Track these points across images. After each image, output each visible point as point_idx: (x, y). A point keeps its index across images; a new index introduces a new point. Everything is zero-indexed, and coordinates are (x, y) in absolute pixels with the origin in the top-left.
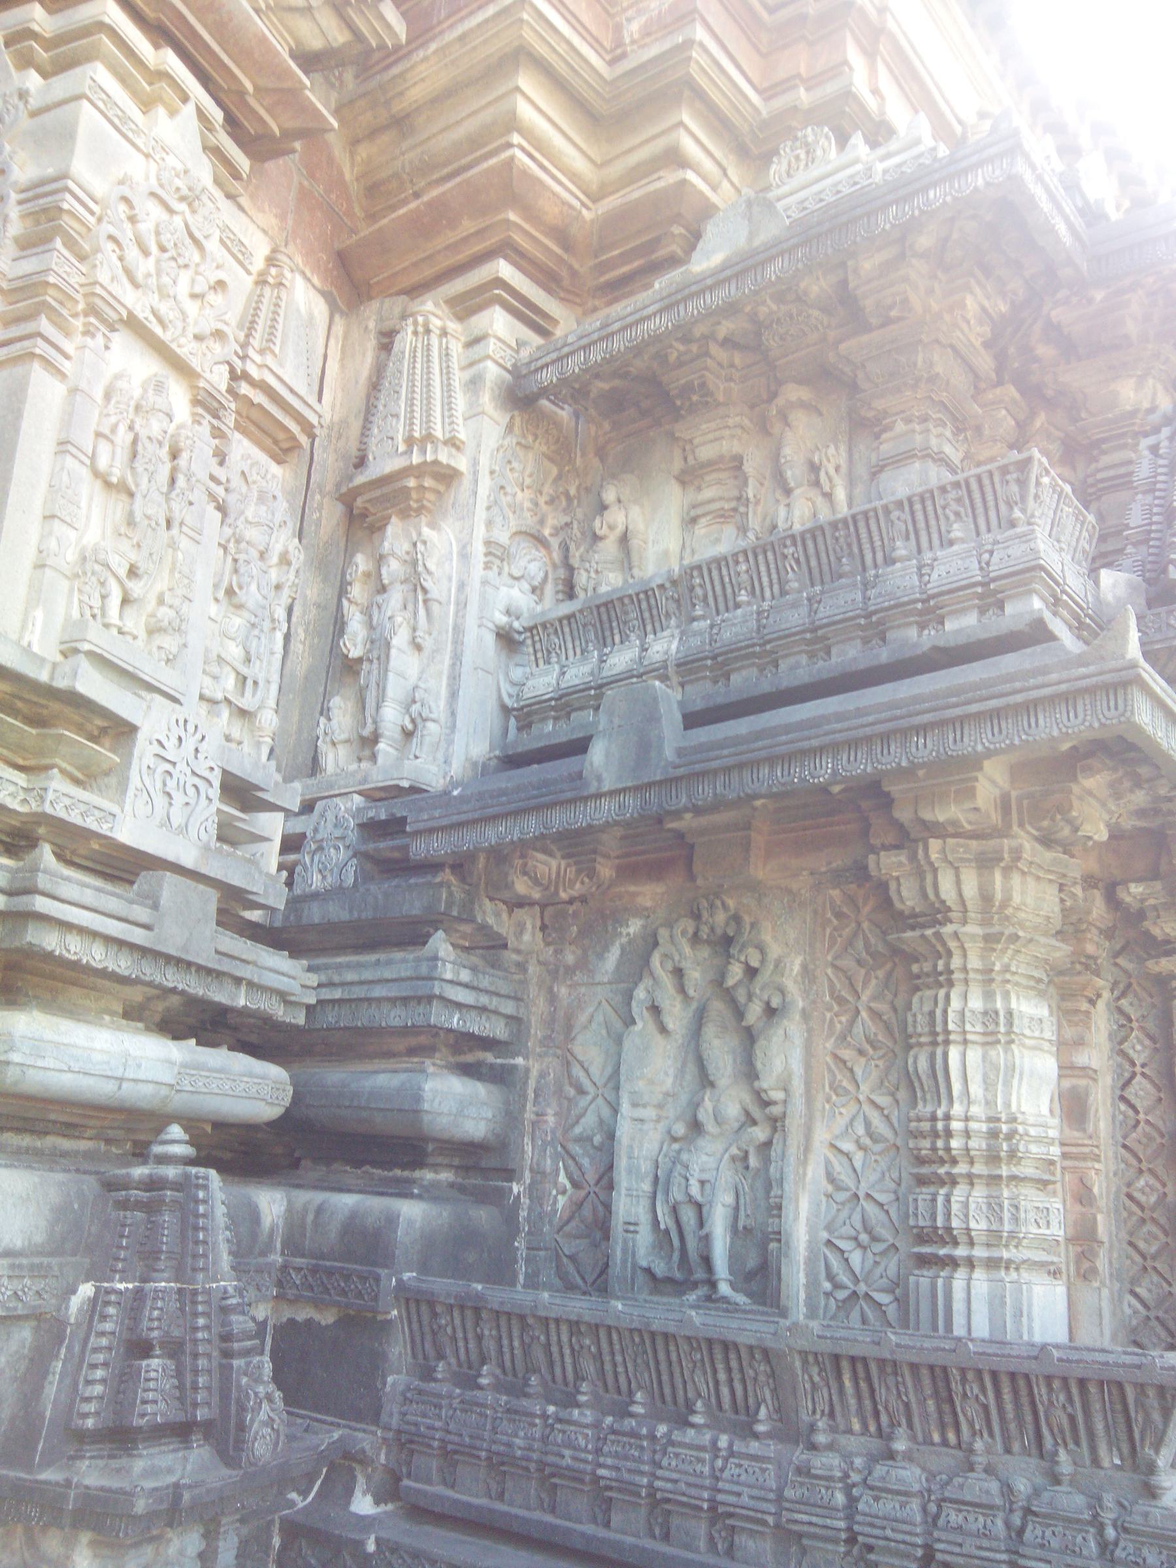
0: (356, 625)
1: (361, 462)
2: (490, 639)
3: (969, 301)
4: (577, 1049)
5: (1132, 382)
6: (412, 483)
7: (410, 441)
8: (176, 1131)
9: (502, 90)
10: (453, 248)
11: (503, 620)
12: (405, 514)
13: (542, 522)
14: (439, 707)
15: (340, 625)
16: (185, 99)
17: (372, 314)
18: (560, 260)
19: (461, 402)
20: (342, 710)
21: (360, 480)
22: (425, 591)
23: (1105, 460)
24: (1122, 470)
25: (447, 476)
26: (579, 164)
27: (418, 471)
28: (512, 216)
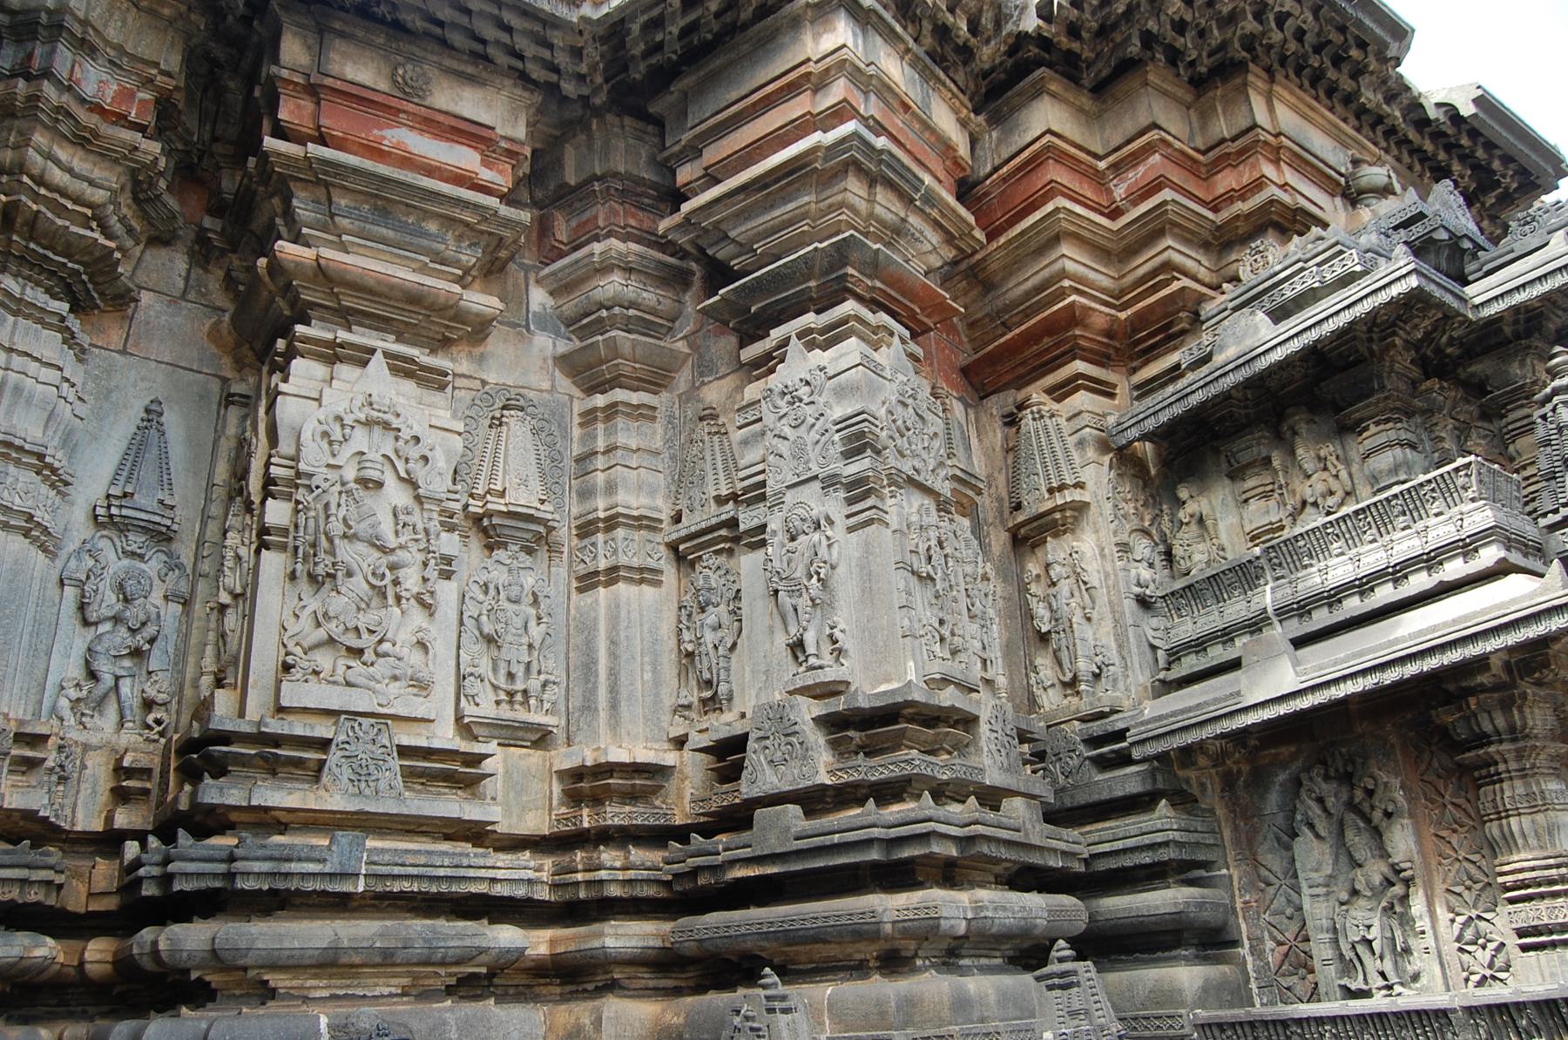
0: (1041, 610)
1: (1018, 507)
2: (1134, 604)
3: (1398, 341)
4: (1260, 858)
5: (1516, 364)
6: (1058, 516)
7: (1051, 491)
8: (1061, 943)
9: (1054, 257)
10: (1040, 354)
11: (1138, 590)
12: (1056, 536)
13: (1142, 519)
14: (1113, 656)
15: (1030, 616)
16: (892, 334)
17: (999, 404)
18: (1107, 345)
19: (1075, 455)
20: (1046, 668)
21: (1021, 518)
22: (1085, 583)
23: (1511, 417)
24: (1525, 422)
25: (1081, 508)
26: (1106, 282)
27: (1061, 508)
28: (1077, 332)
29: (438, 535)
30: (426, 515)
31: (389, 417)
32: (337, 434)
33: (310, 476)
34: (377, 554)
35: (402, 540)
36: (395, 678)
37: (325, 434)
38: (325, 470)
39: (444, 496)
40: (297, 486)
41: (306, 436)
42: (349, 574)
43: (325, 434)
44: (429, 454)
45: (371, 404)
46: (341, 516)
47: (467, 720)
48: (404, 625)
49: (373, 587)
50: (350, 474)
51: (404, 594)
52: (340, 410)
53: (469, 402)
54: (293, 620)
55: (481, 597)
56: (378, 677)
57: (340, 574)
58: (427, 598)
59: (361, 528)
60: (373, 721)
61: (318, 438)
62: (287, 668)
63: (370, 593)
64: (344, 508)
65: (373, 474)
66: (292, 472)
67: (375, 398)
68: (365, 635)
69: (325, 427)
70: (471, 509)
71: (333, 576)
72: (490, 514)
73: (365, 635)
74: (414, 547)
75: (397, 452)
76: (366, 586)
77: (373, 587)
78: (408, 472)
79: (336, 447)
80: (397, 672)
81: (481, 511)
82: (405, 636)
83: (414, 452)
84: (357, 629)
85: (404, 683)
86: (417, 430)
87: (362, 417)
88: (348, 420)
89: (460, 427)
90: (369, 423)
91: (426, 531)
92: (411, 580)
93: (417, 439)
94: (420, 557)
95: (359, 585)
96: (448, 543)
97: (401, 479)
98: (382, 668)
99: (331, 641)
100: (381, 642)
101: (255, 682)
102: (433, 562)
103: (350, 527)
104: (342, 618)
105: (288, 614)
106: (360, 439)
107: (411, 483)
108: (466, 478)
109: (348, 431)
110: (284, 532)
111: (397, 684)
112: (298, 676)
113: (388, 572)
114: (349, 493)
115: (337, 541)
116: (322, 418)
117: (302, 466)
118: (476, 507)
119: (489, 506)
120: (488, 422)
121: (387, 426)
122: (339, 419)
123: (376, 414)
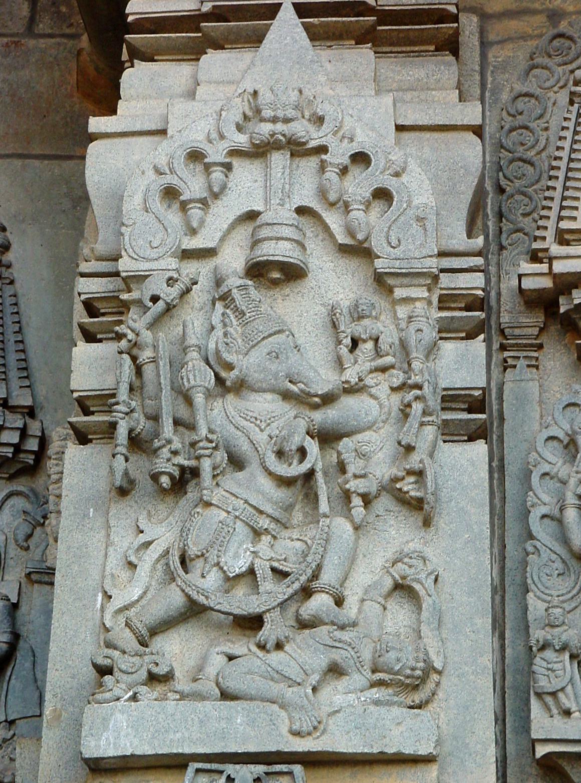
29: (431, 351)
30: (402, 312)
31: (300, 129)
32: (193, 185)
33: (141, 279)
34: (286, 411)
35: (351, 375)
36: (335, 670)
37: (170, 193)
38: (173, 263)
39: (433, 264)
40: (124, 307)
41: (133, 204)
42: (236, 462)
43: (170, 193)
44: (391, 184)
45: (258, 111)
46: (212, 346)
47: (541, 751)
48: (364, 556)
49: (286, 482)
50: (233, 259)
51: (352, 485)
52: (197, 136)
53: (523, 65)
54: (124, 574)
55: (562, 468)
56: (294, 672)
57: (206, 465)
58: (408, 486)
59: (249, 364)
60: (260, 769)
61: (157, 204)
62: (104, 671)
63: (281, 494)
64: (219, 332)
65: (278, 251)
66: (117, 283)
67: (265, 97)
68: (268, 584)
69: (170, 179)
70: (527, 284)
71: (195, 473)
72: (567, 283)
73: (268, 584)
74: (381, 385)
75: (322, 193)
76: (266, 484)
77: (286, 482)
78: (351, 233)
79: (195, 213)
80: (337, 656)
81: (547, 283)
82: (368, 574)
83: (357, 187)
84: (251, 571)
85: (358, 679)
86: (363, 141)
87: (242, 140)
88: (216, 153)
89: (472, 114)
90: (259, 151)
91: (404, 345)
92: (374, 456)
93: (361, 158)
94: (396, 400)
95: (257, 489)
96: (463, 364)
97: (344, 249)
98: (305, 655)
99: (194, 611)
100: (306, 592)
101: (57, 717)
102: (417, 407)
103: (230, 367)
104: (212, 558)
105: (114, 562)
106: (247, 186)
107: (358, 251)
108: (526, 223)
109: (217, 175)
110: (106, 400)
111: (343, 683)
112: (117, 692)
113: (313, 447)
114: (225, 297)
115: (199, 399)
116: (162, 162)
117: (125, 265)
118: (537, 279)
119: (559, 267)
120: (563, 97)
121: (297, 149)
122: (195, 156)
123: (266, 129)
